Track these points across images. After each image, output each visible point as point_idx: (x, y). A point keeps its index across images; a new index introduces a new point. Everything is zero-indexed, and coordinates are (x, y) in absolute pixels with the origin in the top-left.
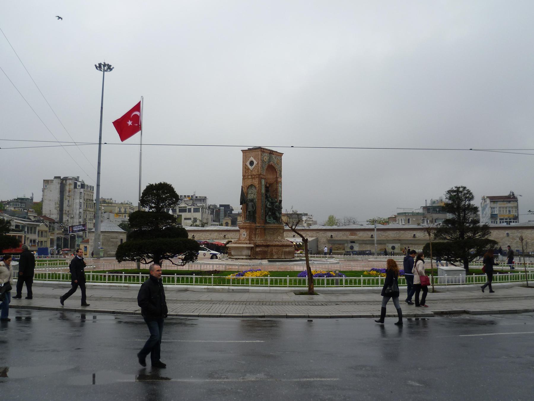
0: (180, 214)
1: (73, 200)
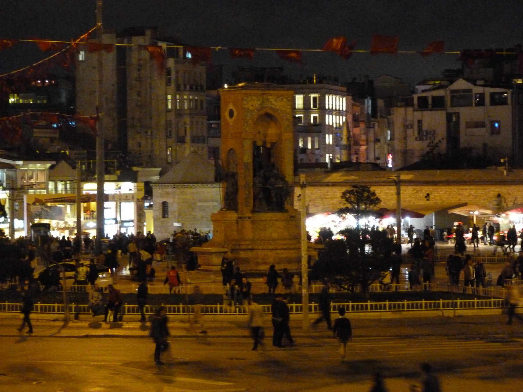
0: (456, 110)
1: (148, 89)
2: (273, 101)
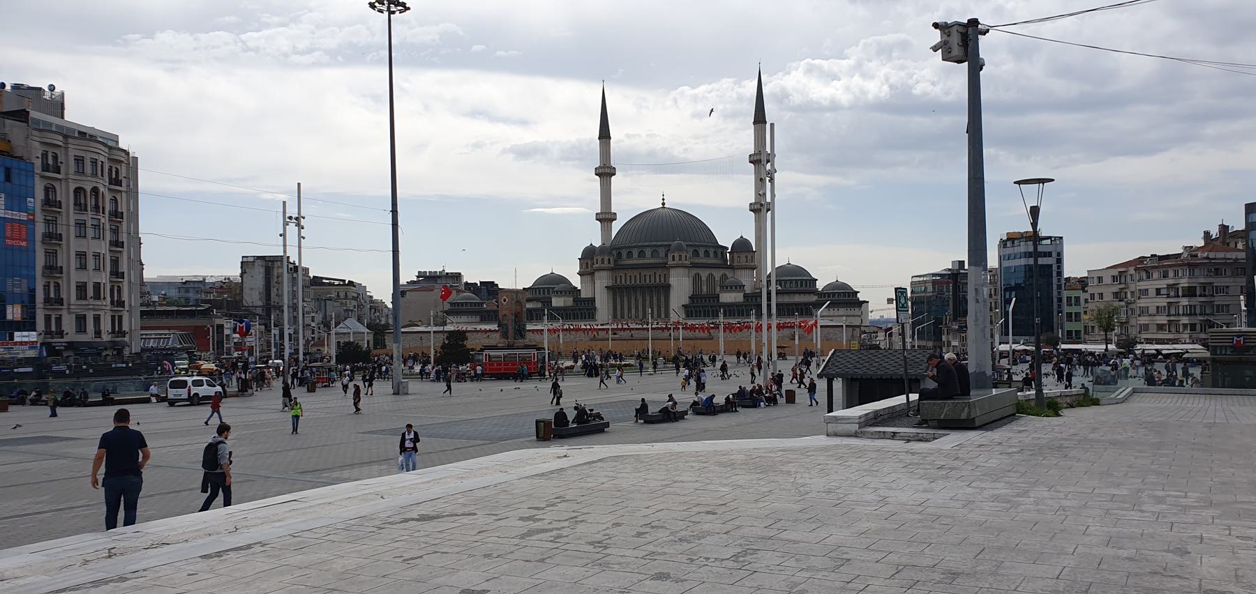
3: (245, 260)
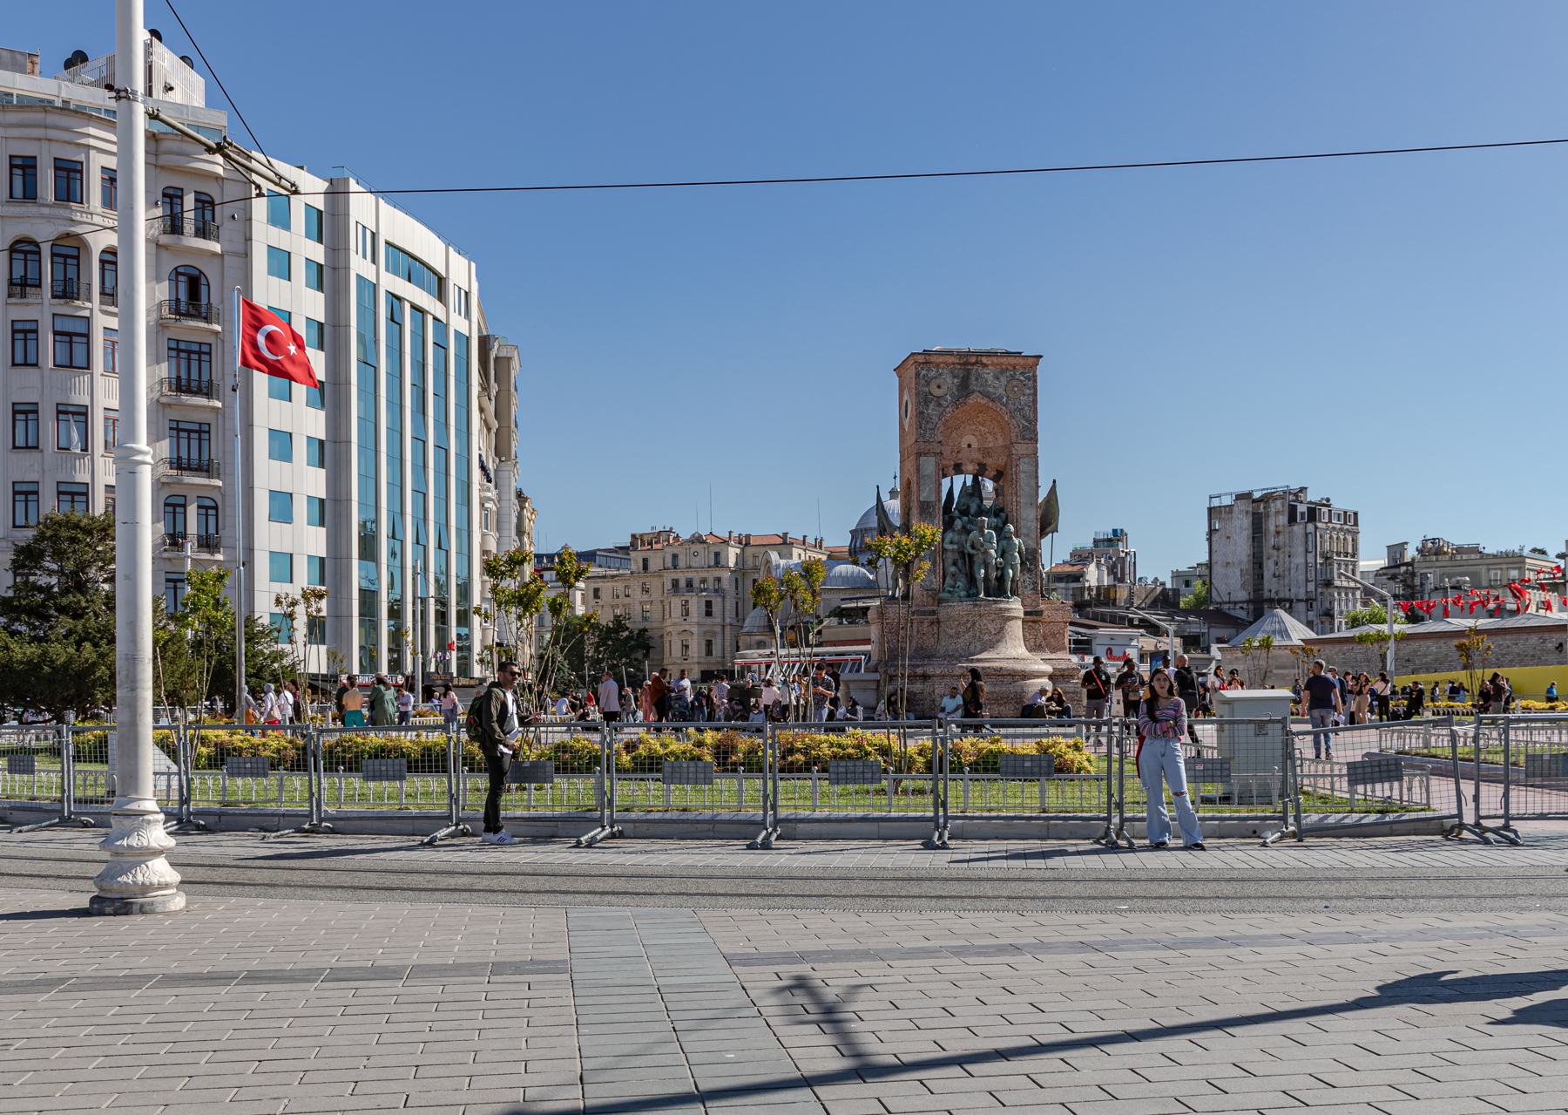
2: (990, 377)
3: (1216, 503)
